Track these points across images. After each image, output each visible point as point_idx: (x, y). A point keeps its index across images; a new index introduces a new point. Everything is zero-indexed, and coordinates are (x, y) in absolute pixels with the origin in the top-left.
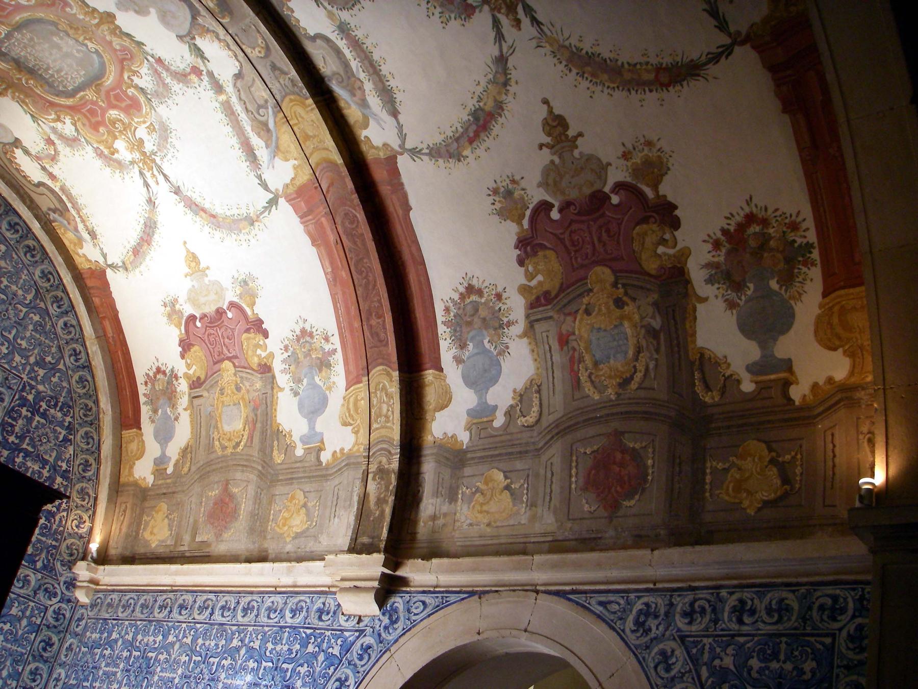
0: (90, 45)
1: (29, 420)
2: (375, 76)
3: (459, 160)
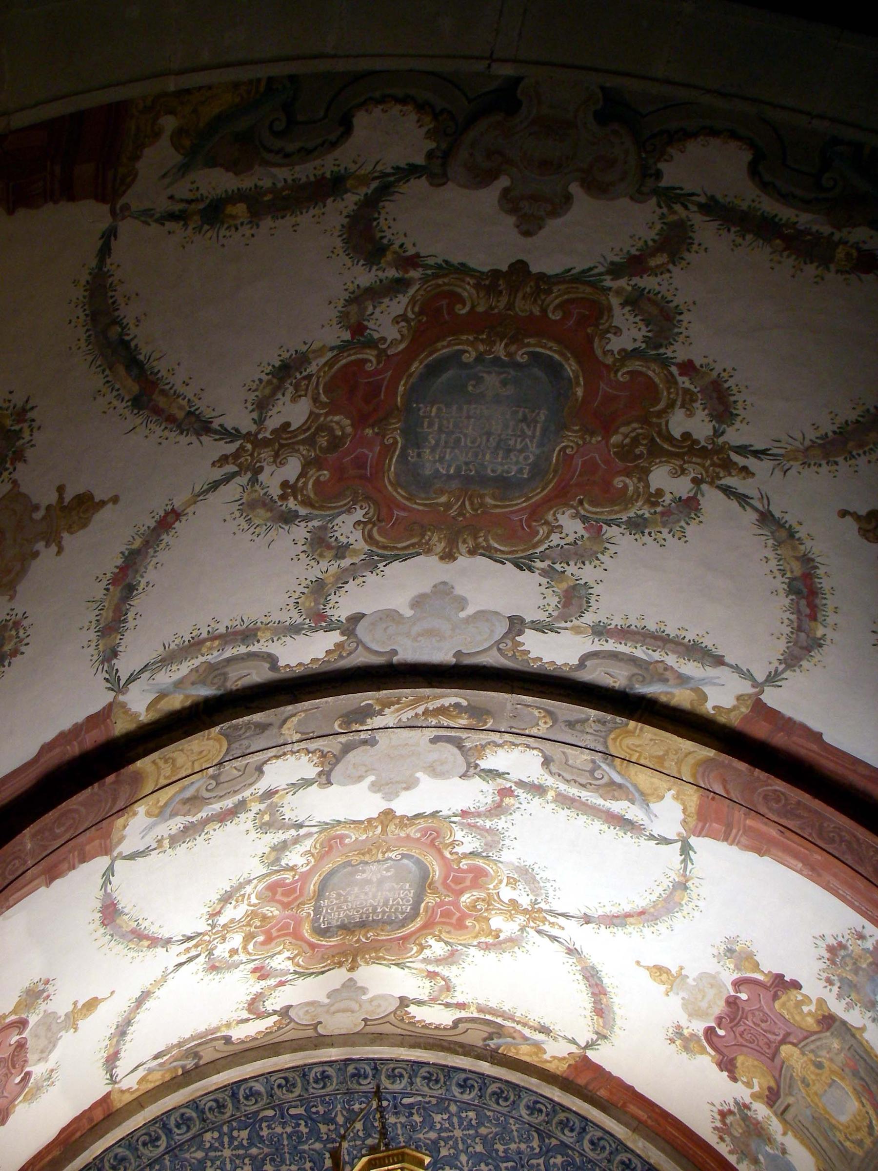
0: (392, 855)
2: (668, 646)
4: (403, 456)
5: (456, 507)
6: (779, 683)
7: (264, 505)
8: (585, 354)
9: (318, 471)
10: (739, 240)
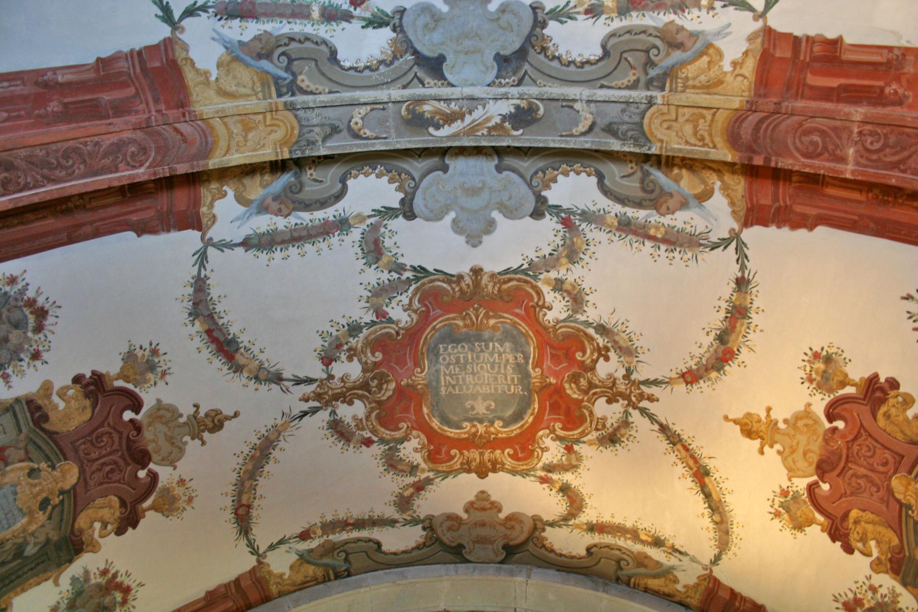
2: (289, 236)
3: (190, 314)
4: (526, 358)
5: (481, 316)
6: (196, 257)
7: (620, 348)
8: (431, 435)
9: (584, 362)
10: (371, 514)
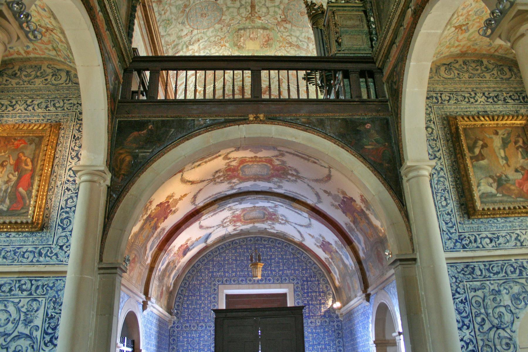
1: (307, 284)
